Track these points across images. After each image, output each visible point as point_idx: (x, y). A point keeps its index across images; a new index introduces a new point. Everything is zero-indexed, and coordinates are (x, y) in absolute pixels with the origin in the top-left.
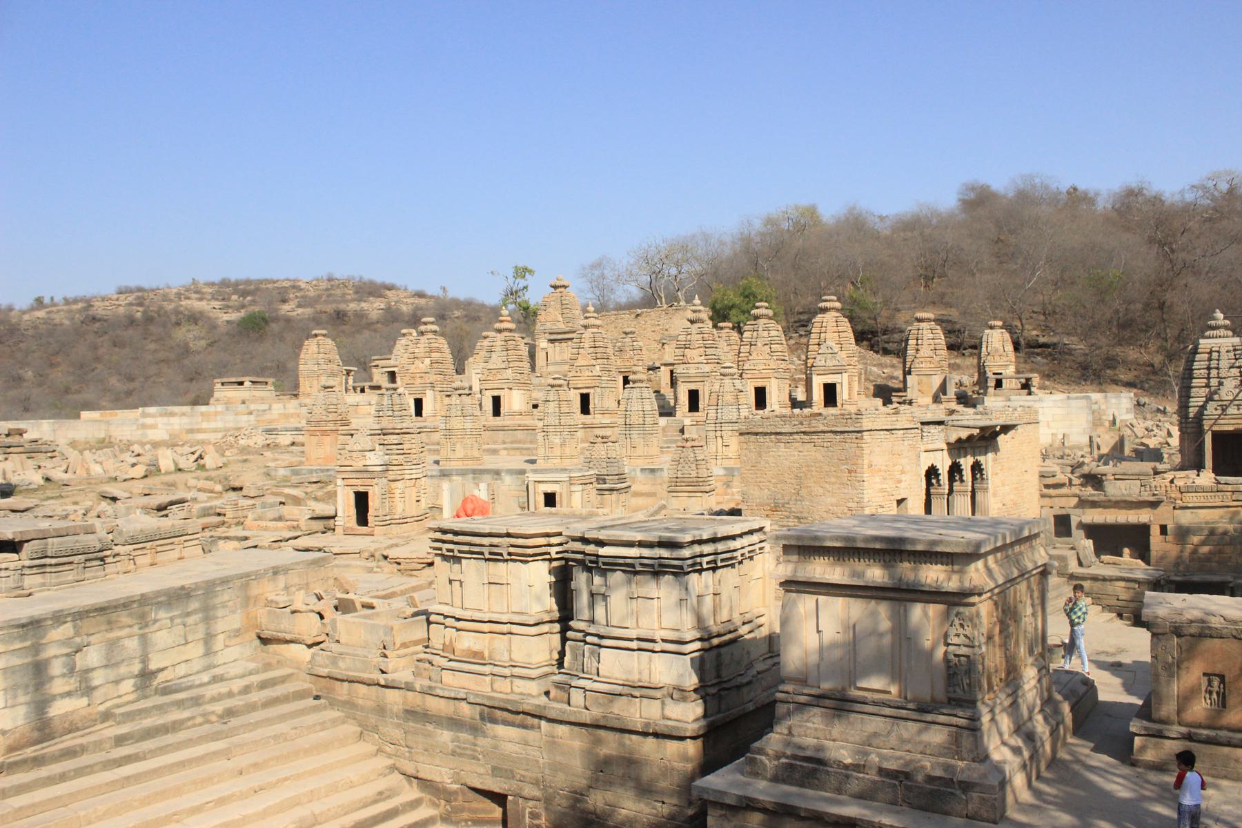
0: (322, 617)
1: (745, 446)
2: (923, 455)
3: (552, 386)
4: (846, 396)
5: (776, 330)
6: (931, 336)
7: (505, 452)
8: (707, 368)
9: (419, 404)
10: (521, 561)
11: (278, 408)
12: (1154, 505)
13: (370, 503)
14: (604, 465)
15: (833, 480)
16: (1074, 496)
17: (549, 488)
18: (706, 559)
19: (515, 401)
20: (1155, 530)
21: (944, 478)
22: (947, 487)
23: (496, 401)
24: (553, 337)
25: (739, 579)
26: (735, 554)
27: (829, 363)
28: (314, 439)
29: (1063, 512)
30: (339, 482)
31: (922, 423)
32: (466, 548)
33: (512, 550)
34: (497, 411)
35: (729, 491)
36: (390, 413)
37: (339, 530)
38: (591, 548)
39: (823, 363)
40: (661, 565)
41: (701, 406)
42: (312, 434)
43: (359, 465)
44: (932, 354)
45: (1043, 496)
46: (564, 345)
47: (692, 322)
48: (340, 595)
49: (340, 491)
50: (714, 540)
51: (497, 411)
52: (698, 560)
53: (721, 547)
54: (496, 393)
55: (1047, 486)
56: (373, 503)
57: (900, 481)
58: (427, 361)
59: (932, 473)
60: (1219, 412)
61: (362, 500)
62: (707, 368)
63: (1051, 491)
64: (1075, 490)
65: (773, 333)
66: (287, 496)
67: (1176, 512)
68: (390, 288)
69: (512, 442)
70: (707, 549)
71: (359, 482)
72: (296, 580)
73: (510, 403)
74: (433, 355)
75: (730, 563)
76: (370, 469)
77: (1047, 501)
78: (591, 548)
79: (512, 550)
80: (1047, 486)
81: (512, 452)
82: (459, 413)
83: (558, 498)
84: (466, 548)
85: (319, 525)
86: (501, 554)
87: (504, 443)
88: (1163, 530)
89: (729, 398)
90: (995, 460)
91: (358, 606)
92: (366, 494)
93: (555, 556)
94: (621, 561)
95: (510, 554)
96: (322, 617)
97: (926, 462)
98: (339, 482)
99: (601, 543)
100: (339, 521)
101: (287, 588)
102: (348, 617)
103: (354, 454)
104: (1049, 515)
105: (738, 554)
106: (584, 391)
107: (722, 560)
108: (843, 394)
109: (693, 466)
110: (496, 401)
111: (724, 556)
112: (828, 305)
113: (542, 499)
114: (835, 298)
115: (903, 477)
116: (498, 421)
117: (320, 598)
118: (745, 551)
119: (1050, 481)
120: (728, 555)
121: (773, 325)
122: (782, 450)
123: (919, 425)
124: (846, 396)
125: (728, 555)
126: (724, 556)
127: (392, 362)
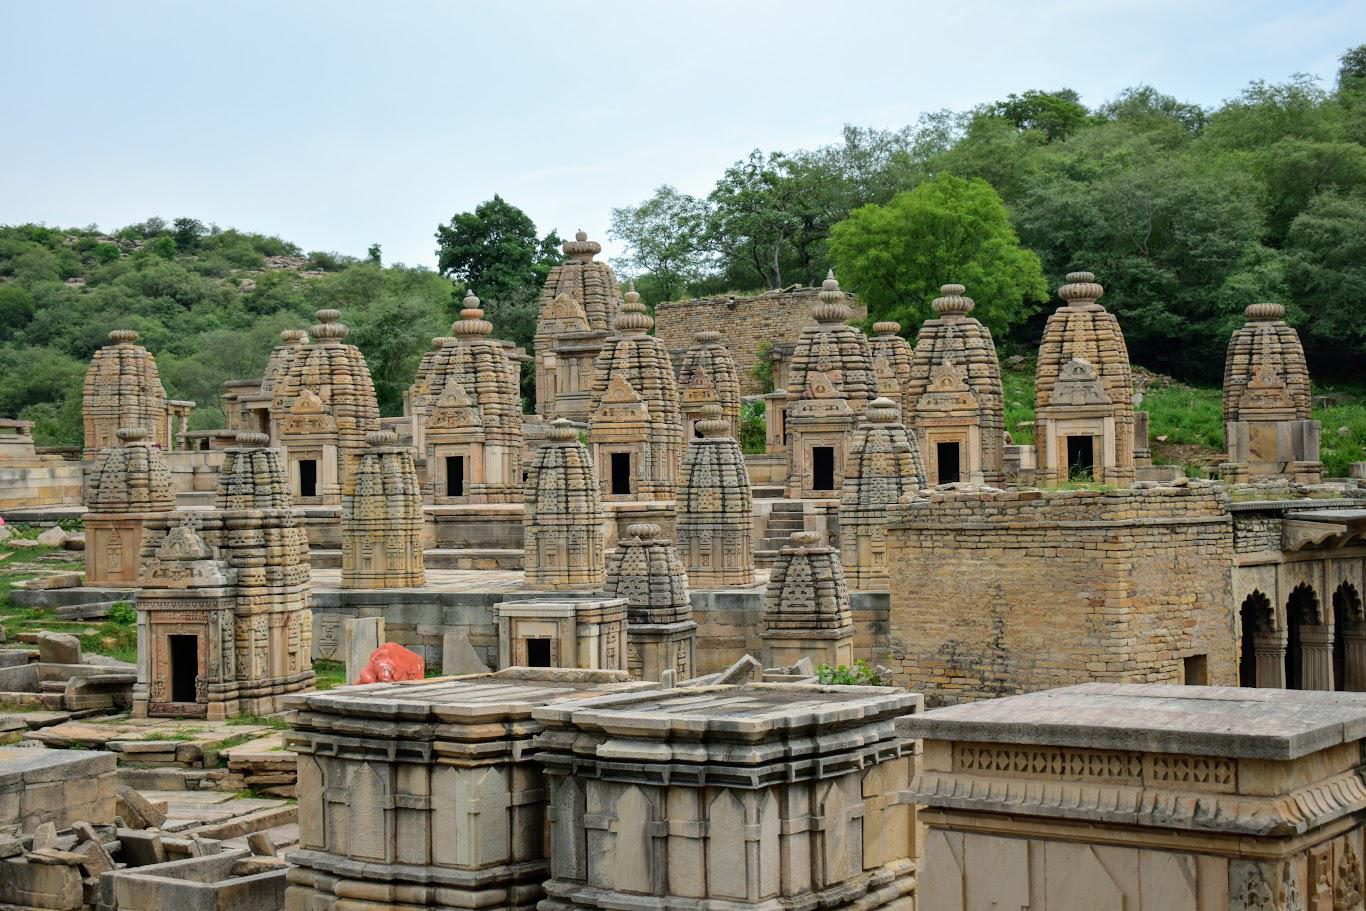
0: (85, 874)
1: (898, 554)
2: (1236, 574)
3: (554, 439)
4: (1110, 460)
5: (979, 338)
6: (1278, 347)
7: (468, 563)
8: (847, 408)
9: (308, 471)
10: (457, 767)
11: (39, 477)
13: (201, 658)
14: (644, 587)
15: (1061, 619)
17: (538, 631)
18: (795, 765)
19: (491, 466)
21: (1280, 619)
22: (1285, 634)
23: (455, 466)
24: (565, 348)
25: (861, 804)
26: (852, 757)
27: (1080, 399)
28: (103, 537)
30: (142, 618)
31: (1235, 513)
32: (355, 742)
33: (439, 746)
34: (455, 487)
35: (882, 638)
36: (249, 488)
37: (139, 708)
38: (581, 744)
39: (1065, 399)
40: (710, 777)
41: (631, 487)
42: (99, 526)
43: (180, 585)
44: (1280, 382)
46: (587, 362)
47: (822, 319)
48: (125, 832)
49: (142, 637)
50: (811, 730)
51: (455, 487)
52: (779, 767)
53: (825, 743)
54: (454, 452)
56: (208, 657)
57: (1192, 624)
58: (326, 390)
59: (1255, 609)
61: (184, 651)
62: (847, 408)
65: (974, 342)
66: (47, 643)
68: (270, 248)
69: (481, 545)
70: (798, 747)
71: (179, 617)
72: (41, 804)
73: (483, 470)
74: (337, 379)
75: (840, 772)
76: (201, 592)
78: (581, 744)
79: (439, 746)
81: (481, 563)
82: (381, 492)
83: (552, 651)
84: (355, 742)
85: (95, 701)
86: (419, 755)
87: (468, 546)
89: (882, 463)
91: (158, 850)
92: (192, 641)
93: (518, 757)
94: (637, 767)
95: (435, 754)
96: (85, 874)
97: (1243, 586)
98: (142, 618)
99: (600, 733)
100: (140, 693)
101: (22, 819)
102: (136, 874)
103: (173, 566)
105: (859, 756)
106: (620, 449)
107: (827, 769)
108: (1106, 454)
109: (810, 592)
110: (455, 466)
111: (830, 760)
112: (1078, 288)
113: (522, 650)
114: (1091, 275)
115: (1198, 616)
116: (456, 506)
117: (83, 837)
118: (875, 750)
120: (841, 758)
121: (974, 326)
122: (967, 562)
123: (1229, 515)
124: (1110, 460)
125: (841, 758)
126: (830, 760)
127: (262, 393)
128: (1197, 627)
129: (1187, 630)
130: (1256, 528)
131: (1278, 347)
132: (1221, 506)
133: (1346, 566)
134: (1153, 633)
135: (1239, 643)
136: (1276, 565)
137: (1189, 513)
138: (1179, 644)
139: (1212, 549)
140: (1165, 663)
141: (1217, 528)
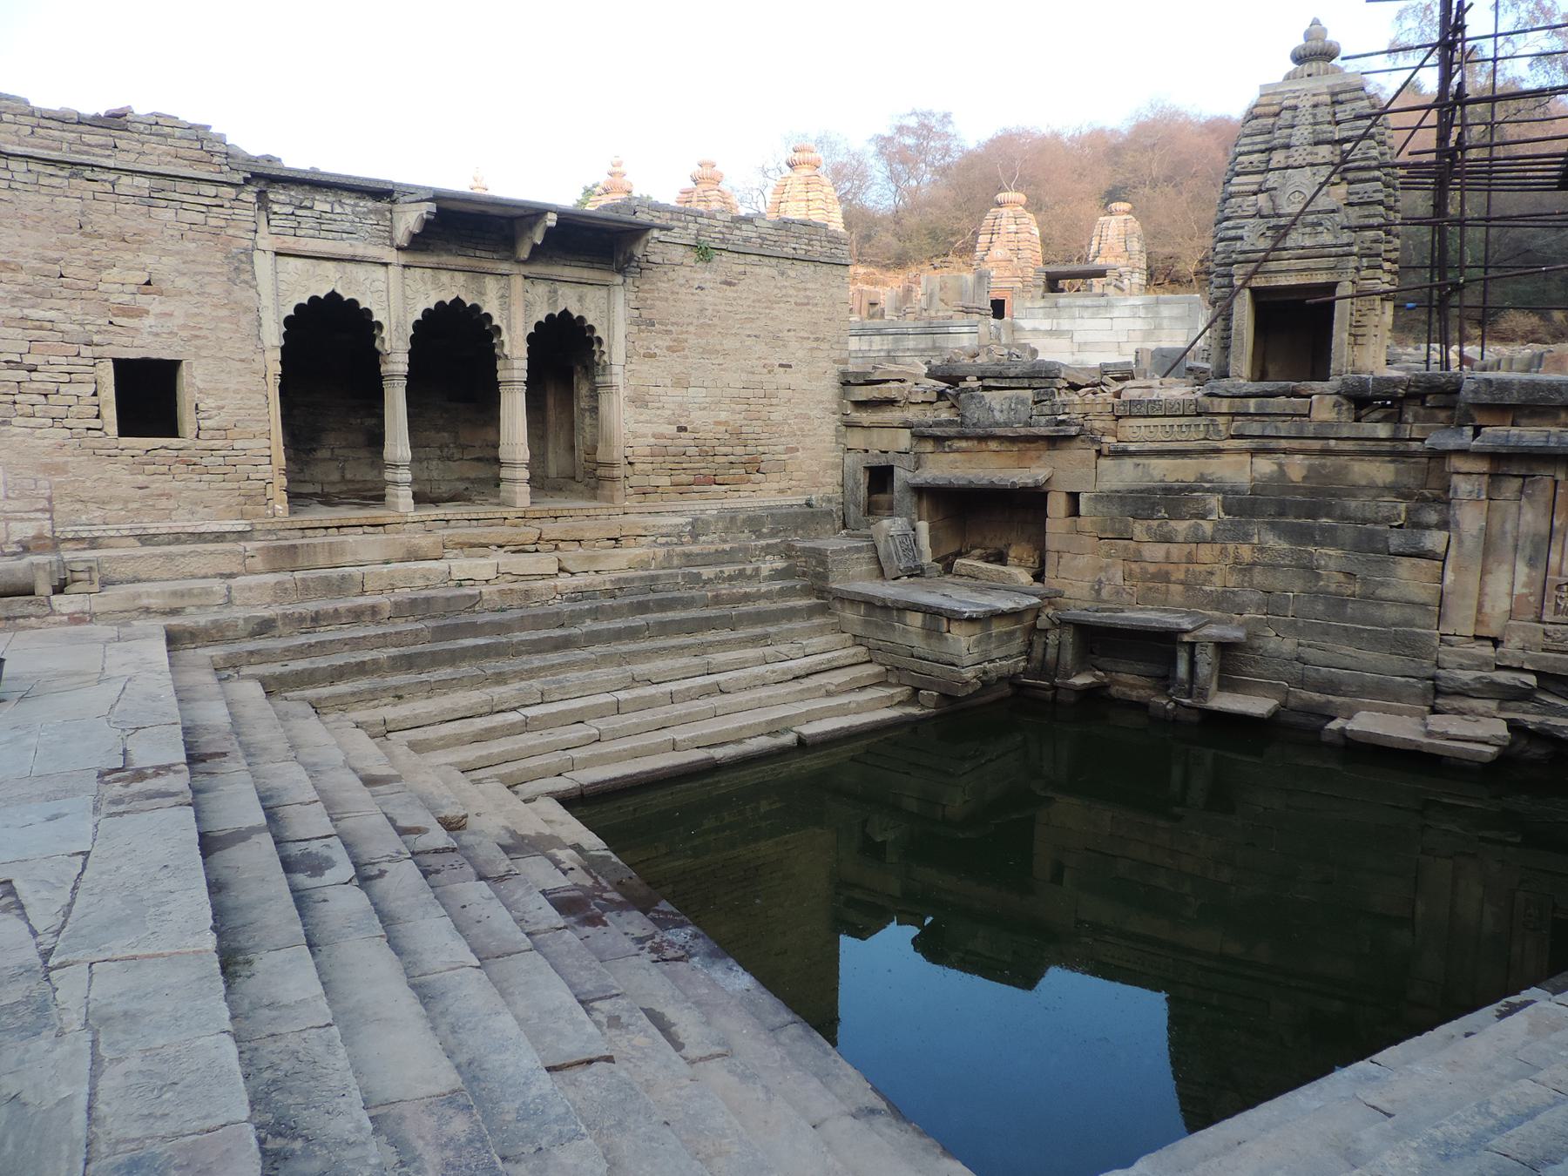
6: (1013, 228)
12: (1055, 441)
16: (907, 425)
20: (1057, 506)
29: (882, 461)
45: (849, 425)
55: (860, 405)
60: (1265, 244)
63: (865, 417)
64: (912, 414)
67: (1103, 462)
77: (856, 439)
80: (860, 405)
88: (1074, 497)
90: (643, 323)
97: (291, 286)
104: (856, 462)
115: (154, 304)
119: (863, 393)
128: (148, 321)
129: (116, 320)
130: (319, 206)
131: (1013, 228)
132: (215, 160)
133: (564, 290)
134: (16, 312)
135: (278, 355)
136: (386, 265)
137: (120, 155)
138: (96, 339)
139: (200, 218)
140: (52, 359)
141: (210, 190)
